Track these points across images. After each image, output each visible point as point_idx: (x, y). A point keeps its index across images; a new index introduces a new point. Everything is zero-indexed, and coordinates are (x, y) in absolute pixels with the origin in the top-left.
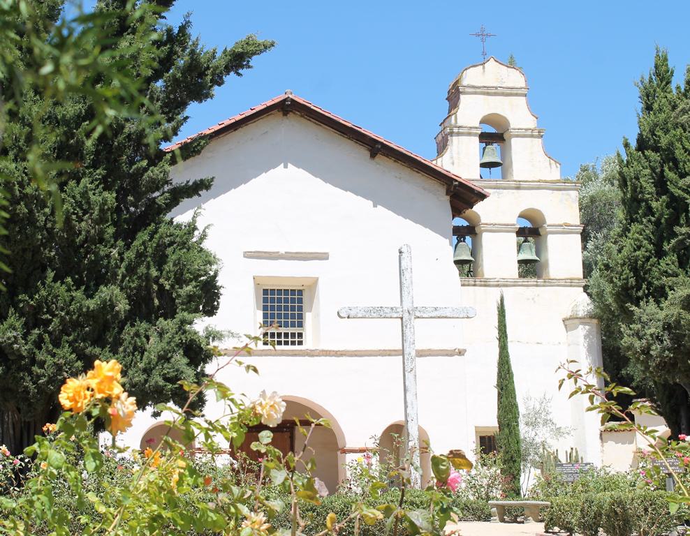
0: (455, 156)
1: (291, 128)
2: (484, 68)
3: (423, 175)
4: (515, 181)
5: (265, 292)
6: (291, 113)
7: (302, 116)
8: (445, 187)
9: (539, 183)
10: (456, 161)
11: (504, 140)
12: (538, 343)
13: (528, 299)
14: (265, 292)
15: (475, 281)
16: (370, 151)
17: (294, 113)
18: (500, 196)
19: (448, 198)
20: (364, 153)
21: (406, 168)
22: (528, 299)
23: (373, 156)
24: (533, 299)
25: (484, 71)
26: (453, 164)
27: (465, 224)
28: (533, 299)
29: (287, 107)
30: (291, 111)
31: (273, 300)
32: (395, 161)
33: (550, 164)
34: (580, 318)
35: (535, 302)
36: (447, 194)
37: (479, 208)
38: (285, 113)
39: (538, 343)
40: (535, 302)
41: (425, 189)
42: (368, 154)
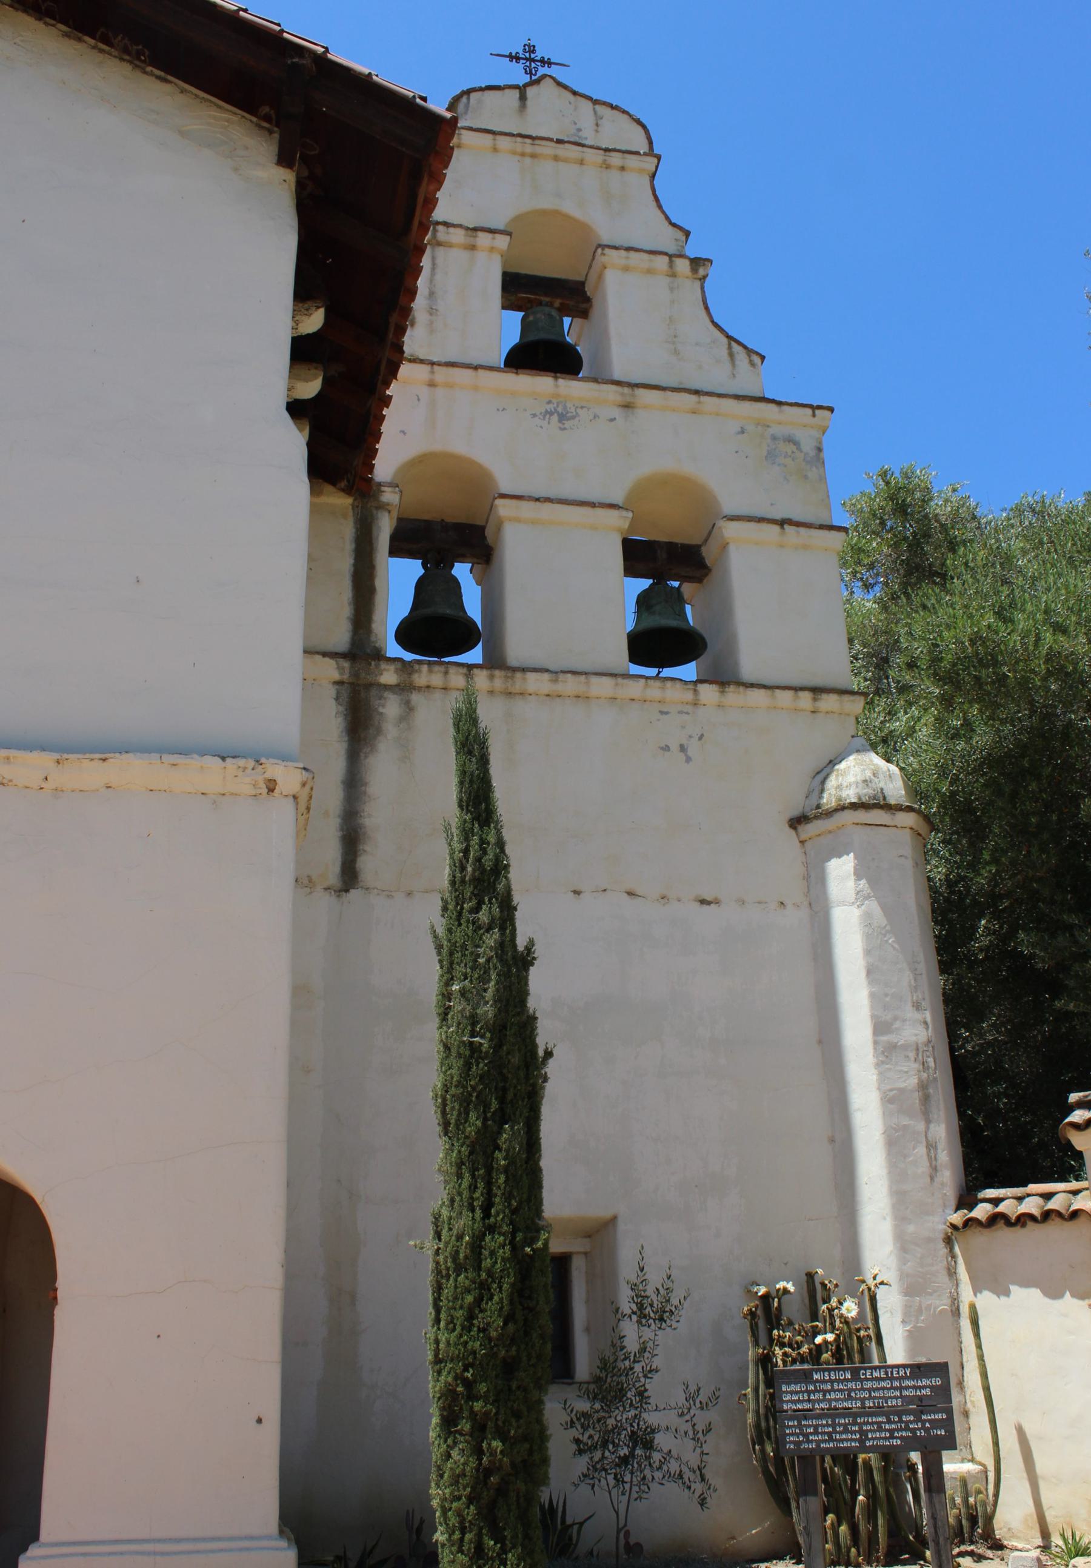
2: (523, 98)
3: (183, 91)
4: (618, 383)
8: (276, 136)
9: (694, 398)
11: (588, 300)
12: (703, 902)
13: (666, 748)
18: (568, 424)
21: (117, 61)
22: (666, 748)
24: (683, 748)
28: (683, 748)
32: (66, 35)
33: (731, 355)
34: (854, 806)
35: (688, 760)
36: (284, 159)
39: (703, 902)
40: (688, 760)
41: (182, 134)
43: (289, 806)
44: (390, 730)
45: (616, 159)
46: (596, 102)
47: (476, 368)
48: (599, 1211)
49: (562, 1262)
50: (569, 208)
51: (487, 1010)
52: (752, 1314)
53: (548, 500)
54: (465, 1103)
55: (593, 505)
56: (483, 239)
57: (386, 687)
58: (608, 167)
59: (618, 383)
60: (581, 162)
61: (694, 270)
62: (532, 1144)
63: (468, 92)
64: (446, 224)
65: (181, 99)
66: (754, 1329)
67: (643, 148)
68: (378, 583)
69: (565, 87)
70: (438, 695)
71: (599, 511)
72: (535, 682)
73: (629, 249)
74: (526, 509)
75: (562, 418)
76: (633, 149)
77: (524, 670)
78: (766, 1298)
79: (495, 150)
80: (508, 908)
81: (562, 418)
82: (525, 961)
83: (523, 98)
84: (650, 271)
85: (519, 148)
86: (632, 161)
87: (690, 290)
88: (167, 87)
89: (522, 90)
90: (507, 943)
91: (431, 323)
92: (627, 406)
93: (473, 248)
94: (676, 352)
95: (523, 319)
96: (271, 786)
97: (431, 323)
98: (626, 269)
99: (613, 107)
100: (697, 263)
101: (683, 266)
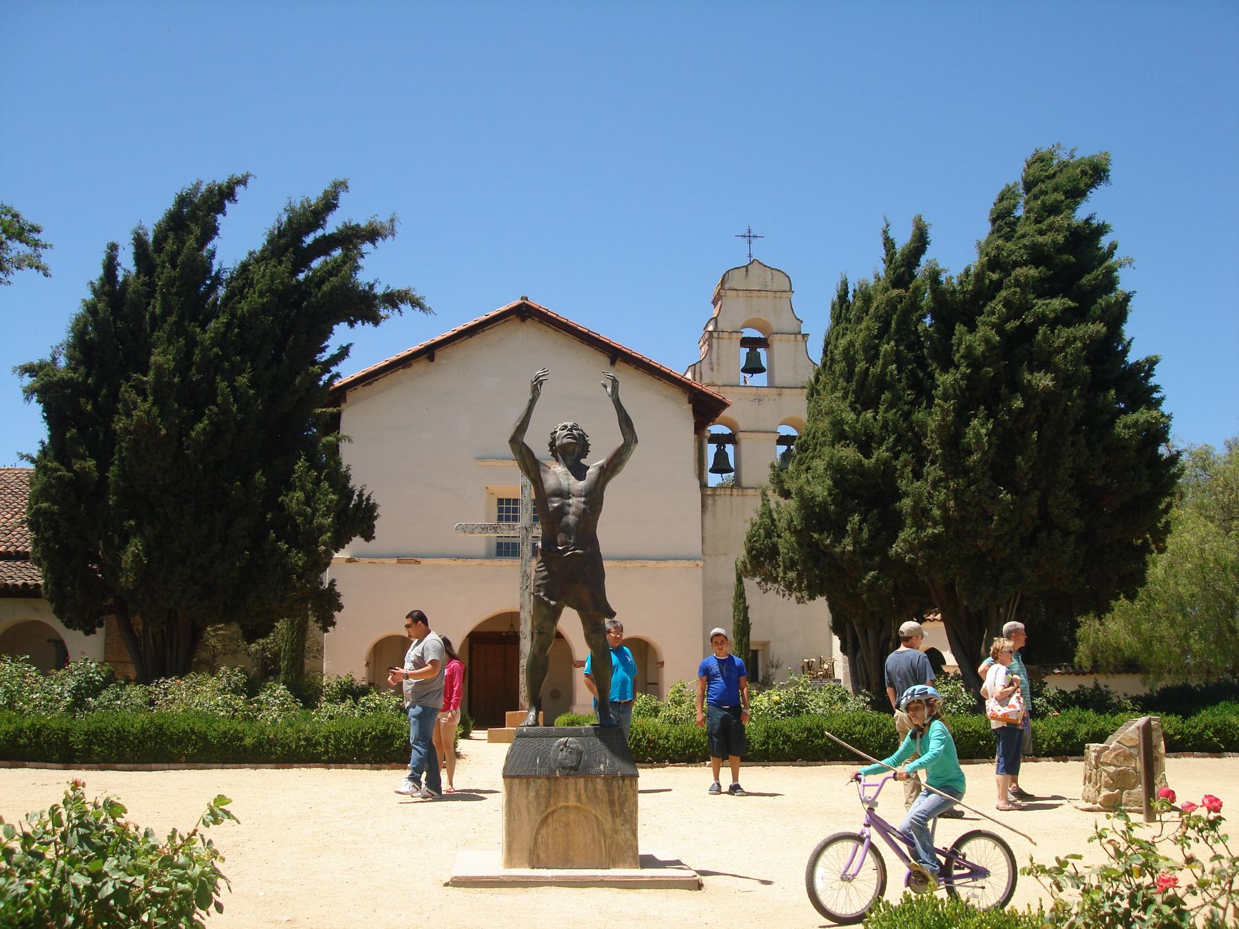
0: (715, 361)
1: (526, 336)
2: (747, 271)
5: (500, 501)
6: (530, 319)
7: (540, 322)
10: (715, 367)
14: (500, 501)
15: (732, 491)
16: (609, 357)
17: (533, 319)
19: (691, 406)
20: (604, 360)
23: (613, 363)
25: (747, 275)
26: (712, 370)
27: (727, 431)
29: (524, 312)
30: (530, 317)
31: (508, 510)
32: (636, 368)
36: (689, 403)
37: (726, 413)
38: (523, 319)
41: (666, 397)
42: (606, 360)
43: (701, 569)
44: (710, 508)
45: (778, 295)
46: (772, 269)
47: (732, 386)
48: (767, 640)
49: (755, 652)
50: (763, 317)
51: (741, 618)
52: (803, 667)
53: (755, 432)
54: (738, 634)
55: (768, 432)
56: (734, 335)
57: (708, 495)
58: (775, 297)
59: (777, 387)
60: (767, 297)
61: (803, 339)
62: (748, 640)
63: (728, 272)
64: (722, 331)
65: (665, 385)
66: (803, 670)
67: (788, 289)
68: (705, 463)
69: (762, 264)
70: (723, 497)
71: (770, 434)
72: (750, 492)
73: (781, 334)
74: (747, 435)
75: (759, 401)
76: (783, 289)
77: (747, 488)
78: (808, 662)
79: (738, 296)
80: (745, 599)
81: (759, 401)
82: (748, 608)
83: (747, 271)
84: (789, 340)
85: (746, 295)
86: (784, 295)
87: (802, 344)
88: (661, 382)
89: (746, 267)
90: (745, 606)
91: (718, 369)
92: (779, 394)
93: (731, 338)
94: (796, 371)
95: (747, 354)
96: (697, 565)
97: (718, 369)
98: (781, 340)
99: (779, 271)
100: (805, 336)
101: (799, 337)
